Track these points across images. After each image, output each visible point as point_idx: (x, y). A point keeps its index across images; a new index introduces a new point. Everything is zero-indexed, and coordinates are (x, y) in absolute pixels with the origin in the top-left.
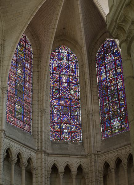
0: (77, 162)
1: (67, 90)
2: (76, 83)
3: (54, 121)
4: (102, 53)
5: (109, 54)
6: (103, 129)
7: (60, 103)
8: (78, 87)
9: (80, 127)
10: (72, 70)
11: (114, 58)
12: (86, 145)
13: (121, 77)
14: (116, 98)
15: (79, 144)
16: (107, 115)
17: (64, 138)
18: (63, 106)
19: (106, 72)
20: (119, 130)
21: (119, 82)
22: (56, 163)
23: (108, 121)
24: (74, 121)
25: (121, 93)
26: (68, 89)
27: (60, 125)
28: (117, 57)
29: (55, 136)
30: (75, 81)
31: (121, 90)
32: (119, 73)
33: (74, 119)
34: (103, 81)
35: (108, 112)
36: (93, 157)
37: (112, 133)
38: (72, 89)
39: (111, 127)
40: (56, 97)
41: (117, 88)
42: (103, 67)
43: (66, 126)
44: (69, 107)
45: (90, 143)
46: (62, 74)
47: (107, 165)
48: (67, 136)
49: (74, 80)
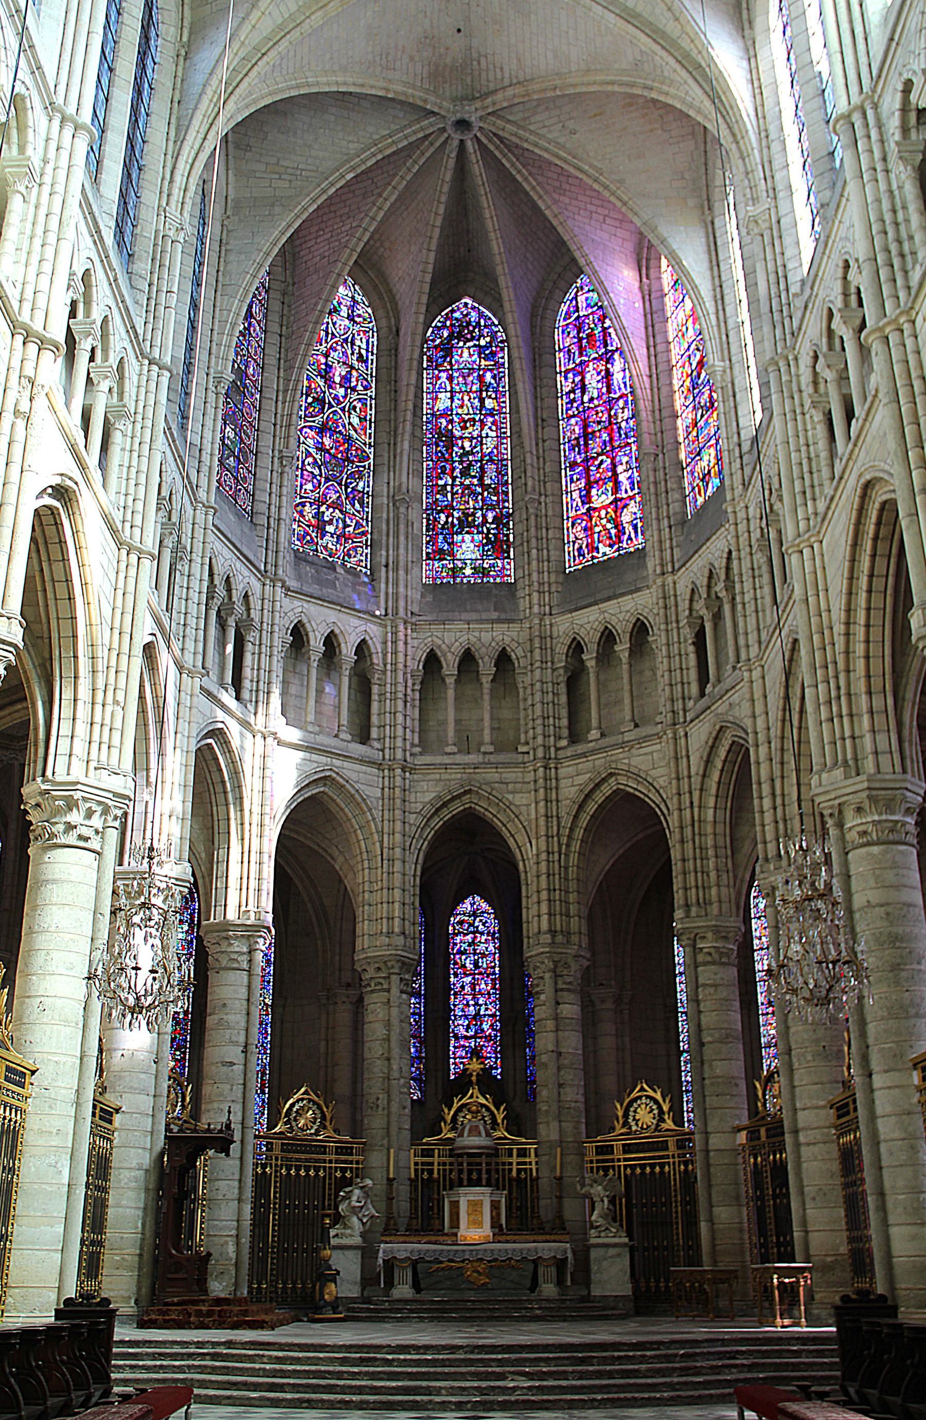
0: (357, 630)
1: (343, 409)
6: (427, 554)
7: (323, 443)
10: (360, 353)
13: (494, 423)
14: (474, 477)
16: (443, 517)
17: (326, 548)
18: (328, 451)
19: (451, 391)
20: (475, 568)
21: (487, 436)
22: (305, 621)
24: (353, 506)
25: (491, 469)
30: (366, 388)
31: (491, 461)
33: (354, 499)
34: (441, 416)
35: (449, 509)
36: (401, 628)
37: (455, 572)
38: (354, 408)
39: (452, 554)
45: (396, 584)
47: (432, 661)
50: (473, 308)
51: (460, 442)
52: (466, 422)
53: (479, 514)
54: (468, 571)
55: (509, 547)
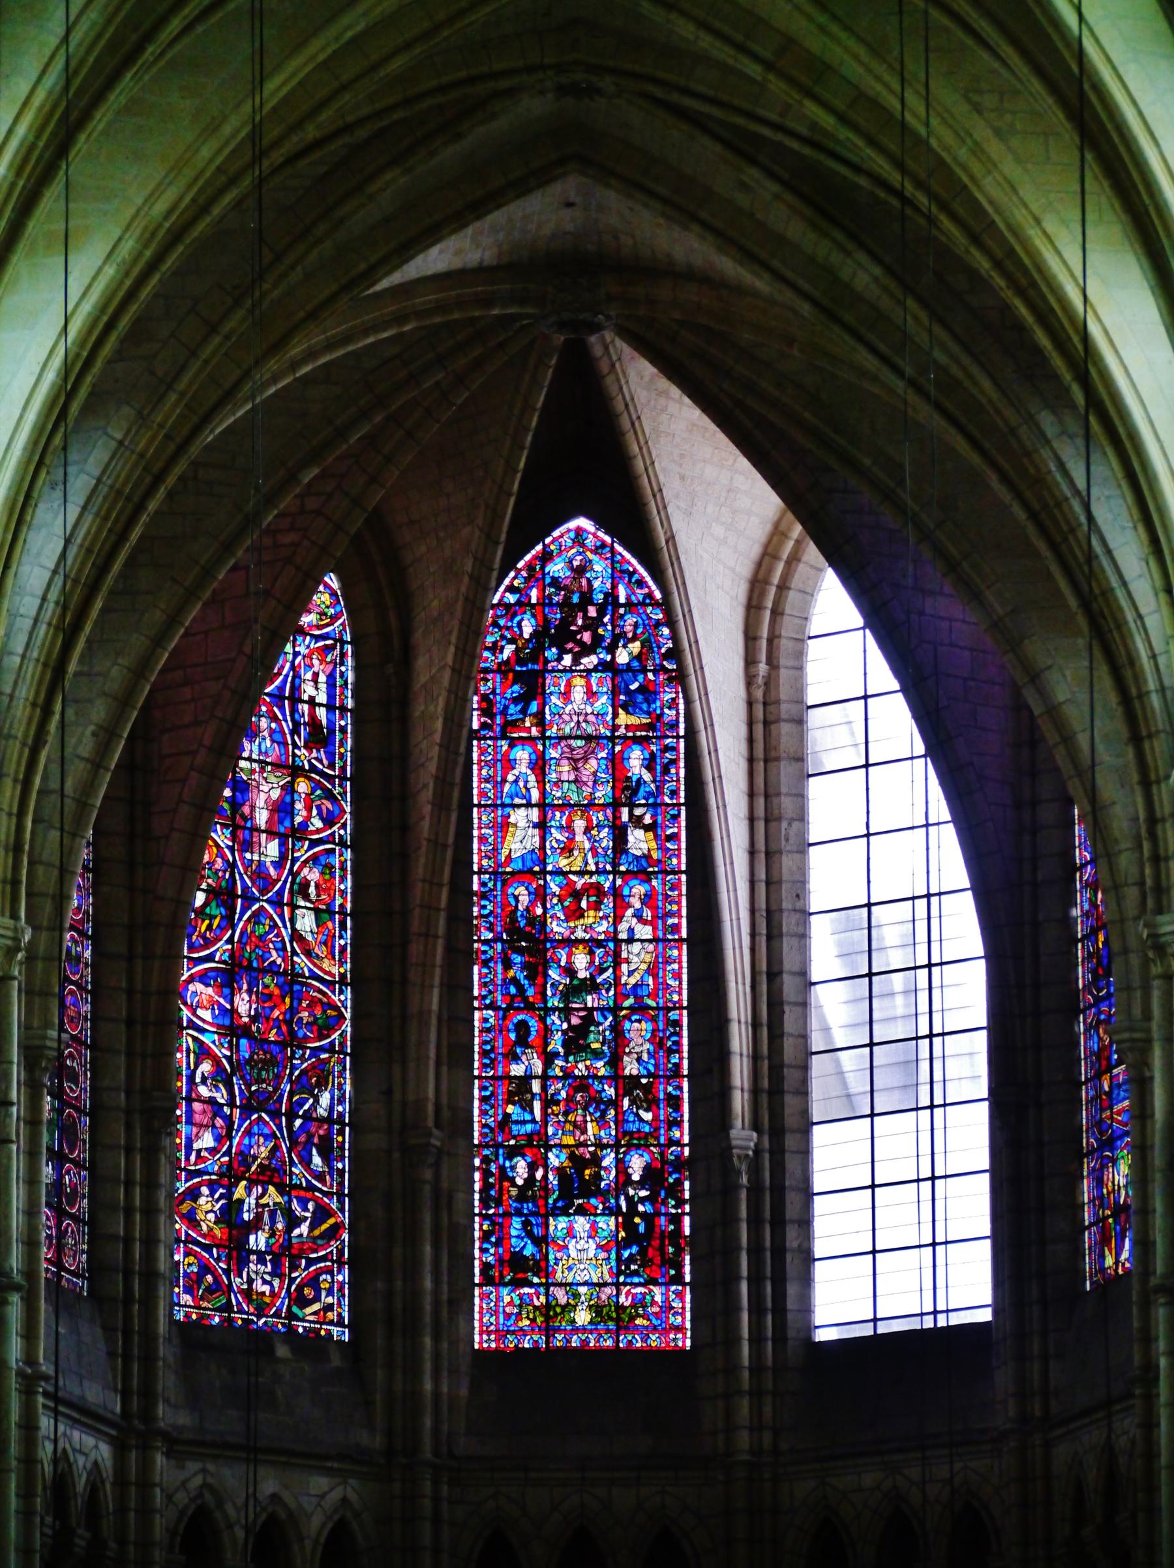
1: (277, 903)
2: (330, 839)
3: (193, 1158)
4: (527, 630)
5: (576, 661)
6: (485, 1267)
7: (233, 1012)
8: (343, 879)
9: (342, 1210)
10: (314, 722)
11: (615, 715)
12: (380, 1375)
13: (648, 899)
14: (597, 1055)
15: (336, 1360)
17: (248, 1294)
18: (245, 1032)
20: (597, 1309)
21: (631, 940)
23: (532, 1214)
24: (307, 1162)
25: (638, 1032)
26: (280, 892)
27: (229, 1195)
28: (633, 720)
29: (200, 1277)
30: (329, 821)
31: (640, 1009)
32: (637, 858)
33: (309, 1144)
35: (537, 1144)
39: (541, 1266)
40: (210, 958)
41: (617, 978)
42: (522, 755)
43: (263, 1201)
44: (283, 1045)
45: (413, 1370)
46: (249, 759)
48: (265, 1282)
49: (320, 814)
50: (600, 548)
51: (562, 955)
52: (577, 895)
53: (609, 1160)
54: (582, 1317)
55: (679, 1252)
